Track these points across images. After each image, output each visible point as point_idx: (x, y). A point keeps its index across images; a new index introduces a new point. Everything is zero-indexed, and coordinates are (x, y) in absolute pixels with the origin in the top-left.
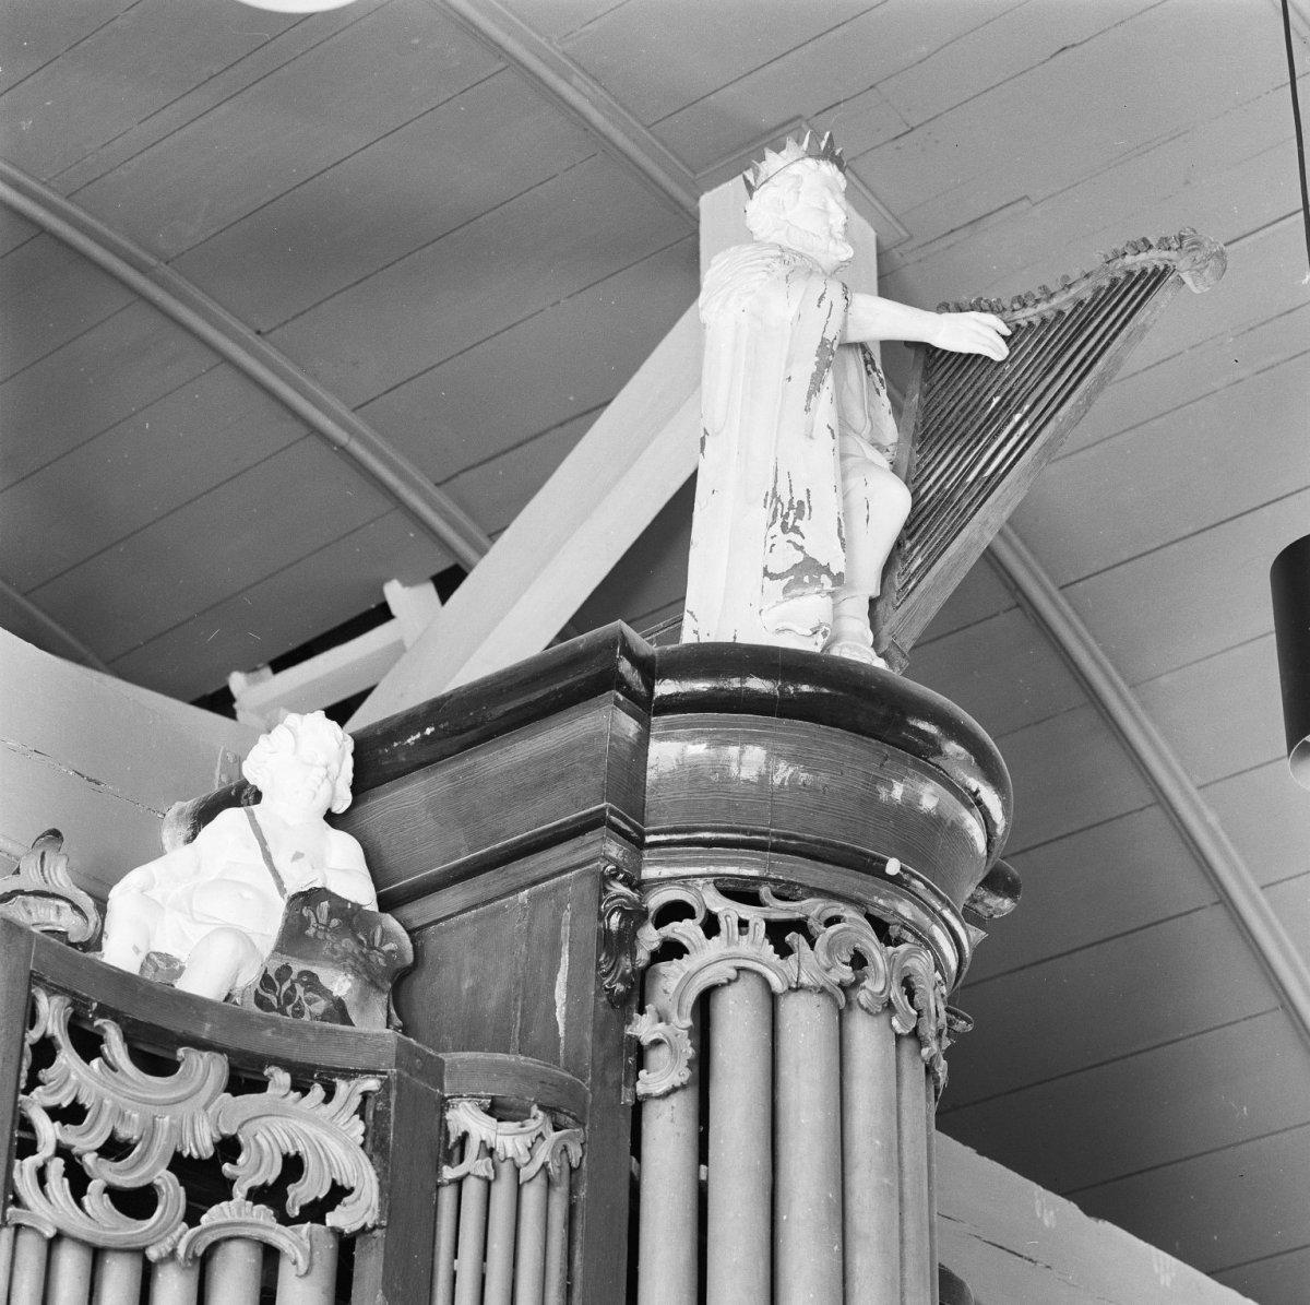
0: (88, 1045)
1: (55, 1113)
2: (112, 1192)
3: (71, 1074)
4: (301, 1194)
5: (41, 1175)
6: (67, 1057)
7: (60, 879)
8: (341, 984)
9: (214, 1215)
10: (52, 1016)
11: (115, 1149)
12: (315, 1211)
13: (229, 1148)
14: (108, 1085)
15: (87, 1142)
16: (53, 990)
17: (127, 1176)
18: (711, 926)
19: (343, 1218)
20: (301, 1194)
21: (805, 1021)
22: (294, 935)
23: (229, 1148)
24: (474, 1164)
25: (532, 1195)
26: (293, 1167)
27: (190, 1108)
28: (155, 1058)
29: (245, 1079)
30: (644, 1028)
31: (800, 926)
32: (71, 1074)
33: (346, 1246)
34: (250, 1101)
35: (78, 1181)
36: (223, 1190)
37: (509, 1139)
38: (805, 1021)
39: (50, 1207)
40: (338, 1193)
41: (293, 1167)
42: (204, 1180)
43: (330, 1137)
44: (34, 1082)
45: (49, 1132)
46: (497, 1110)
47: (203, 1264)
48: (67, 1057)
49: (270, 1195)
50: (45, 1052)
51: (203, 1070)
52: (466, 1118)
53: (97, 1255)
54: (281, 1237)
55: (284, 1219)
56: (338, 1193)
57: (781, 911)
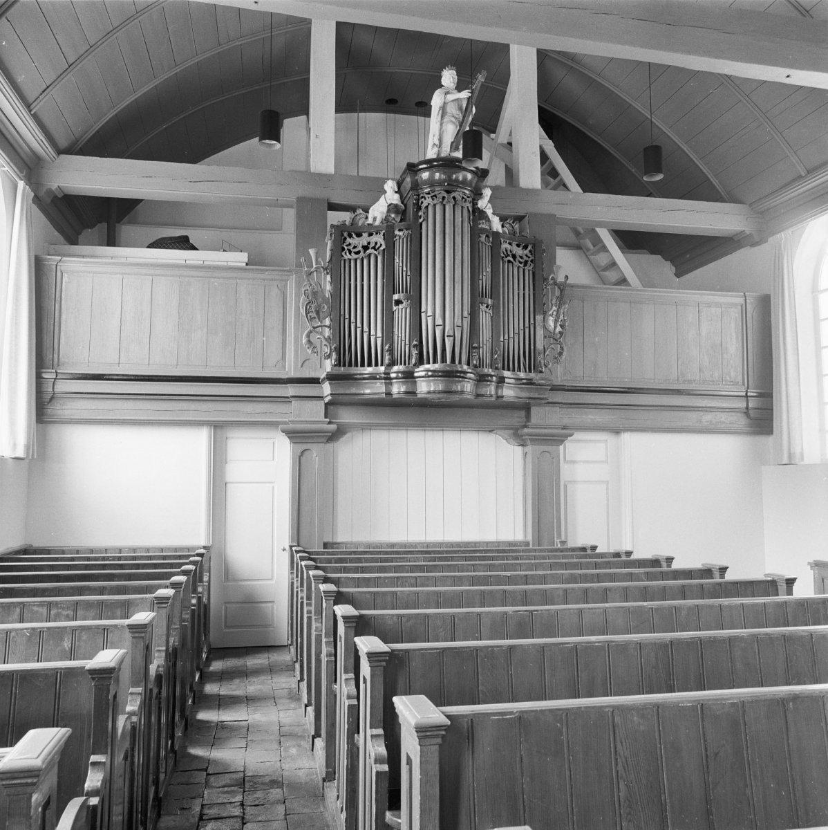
0: (350, 236)
1: (347, 246)
2: (354, 253)
3: (349, 240)
4: (377, 247)
5: (346, 253)
6: (348, 239)
7: (361, 211)
8: (393, 216)
9: (368, 252)
10: (346, 234)
11: (355, 247)
12: (379, 248)
13: (369, 243)
14: (354, 241)
15: (351, 248)
16: (345, 231)
17: (356, 250)
18: (425, 199)
19: (382, 248)
20: (377, 247)
21: (439, 208)
22: (389, 211)
23: (369, 243)
24: (397, 238)
25: (405, 239)
26: (376, 243)
27: (364, 240)
28: (359, 235)
29: (370, 235)
30: (420, 214)
31: (435, 196)
32: (349, 240)
33: (384, 250)
34: (371, 237)
35: (350, 252)
36: (368, 248)
37: (401, 233)
38: (439, 208)
39: (347, 256)
40: (381, 245)
41: (376, 243)
42: (365, 248)
43: (379, 239)
44: (344, 242)
45: (346, 248)
46: (400, 230)
47: (369, 255)
48: (348, 239)
49: (374, 248)
50: (345, 239)
51: (365, 235)
52: (397, 232)
53: (356, 260)
54: (375, 252)
55: (376, 250)
56: (381, 245)
57: (433, 194)
